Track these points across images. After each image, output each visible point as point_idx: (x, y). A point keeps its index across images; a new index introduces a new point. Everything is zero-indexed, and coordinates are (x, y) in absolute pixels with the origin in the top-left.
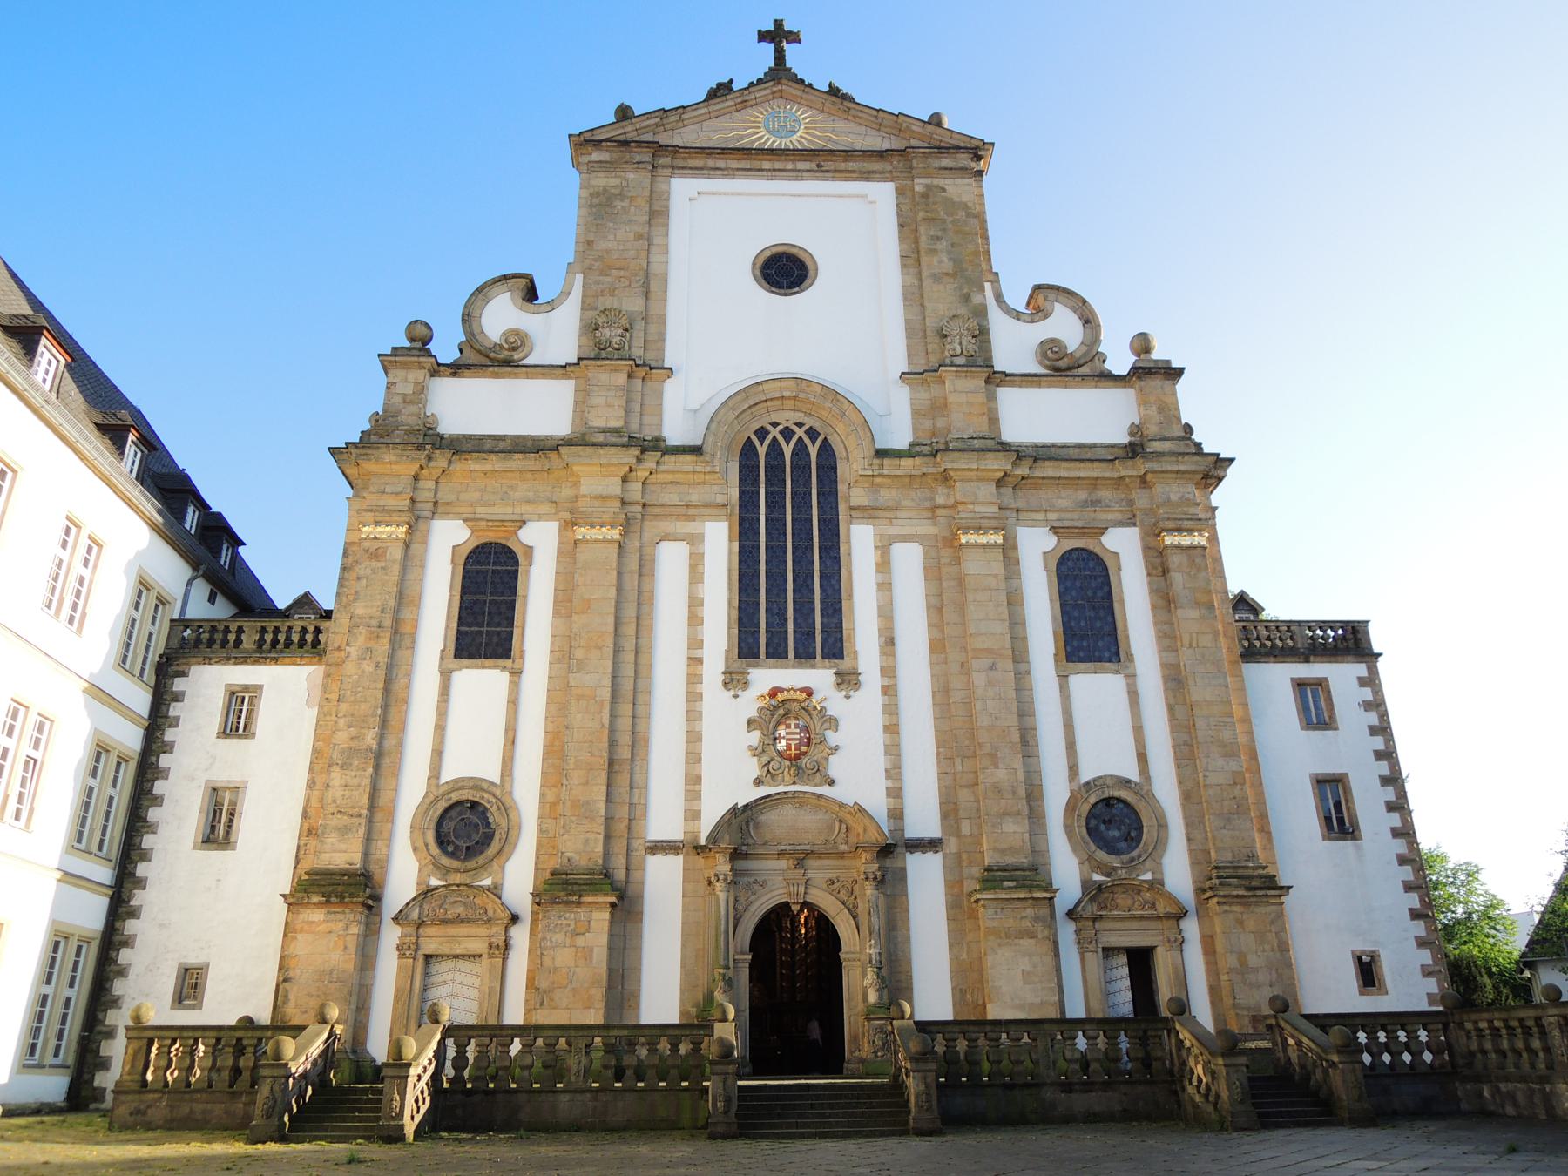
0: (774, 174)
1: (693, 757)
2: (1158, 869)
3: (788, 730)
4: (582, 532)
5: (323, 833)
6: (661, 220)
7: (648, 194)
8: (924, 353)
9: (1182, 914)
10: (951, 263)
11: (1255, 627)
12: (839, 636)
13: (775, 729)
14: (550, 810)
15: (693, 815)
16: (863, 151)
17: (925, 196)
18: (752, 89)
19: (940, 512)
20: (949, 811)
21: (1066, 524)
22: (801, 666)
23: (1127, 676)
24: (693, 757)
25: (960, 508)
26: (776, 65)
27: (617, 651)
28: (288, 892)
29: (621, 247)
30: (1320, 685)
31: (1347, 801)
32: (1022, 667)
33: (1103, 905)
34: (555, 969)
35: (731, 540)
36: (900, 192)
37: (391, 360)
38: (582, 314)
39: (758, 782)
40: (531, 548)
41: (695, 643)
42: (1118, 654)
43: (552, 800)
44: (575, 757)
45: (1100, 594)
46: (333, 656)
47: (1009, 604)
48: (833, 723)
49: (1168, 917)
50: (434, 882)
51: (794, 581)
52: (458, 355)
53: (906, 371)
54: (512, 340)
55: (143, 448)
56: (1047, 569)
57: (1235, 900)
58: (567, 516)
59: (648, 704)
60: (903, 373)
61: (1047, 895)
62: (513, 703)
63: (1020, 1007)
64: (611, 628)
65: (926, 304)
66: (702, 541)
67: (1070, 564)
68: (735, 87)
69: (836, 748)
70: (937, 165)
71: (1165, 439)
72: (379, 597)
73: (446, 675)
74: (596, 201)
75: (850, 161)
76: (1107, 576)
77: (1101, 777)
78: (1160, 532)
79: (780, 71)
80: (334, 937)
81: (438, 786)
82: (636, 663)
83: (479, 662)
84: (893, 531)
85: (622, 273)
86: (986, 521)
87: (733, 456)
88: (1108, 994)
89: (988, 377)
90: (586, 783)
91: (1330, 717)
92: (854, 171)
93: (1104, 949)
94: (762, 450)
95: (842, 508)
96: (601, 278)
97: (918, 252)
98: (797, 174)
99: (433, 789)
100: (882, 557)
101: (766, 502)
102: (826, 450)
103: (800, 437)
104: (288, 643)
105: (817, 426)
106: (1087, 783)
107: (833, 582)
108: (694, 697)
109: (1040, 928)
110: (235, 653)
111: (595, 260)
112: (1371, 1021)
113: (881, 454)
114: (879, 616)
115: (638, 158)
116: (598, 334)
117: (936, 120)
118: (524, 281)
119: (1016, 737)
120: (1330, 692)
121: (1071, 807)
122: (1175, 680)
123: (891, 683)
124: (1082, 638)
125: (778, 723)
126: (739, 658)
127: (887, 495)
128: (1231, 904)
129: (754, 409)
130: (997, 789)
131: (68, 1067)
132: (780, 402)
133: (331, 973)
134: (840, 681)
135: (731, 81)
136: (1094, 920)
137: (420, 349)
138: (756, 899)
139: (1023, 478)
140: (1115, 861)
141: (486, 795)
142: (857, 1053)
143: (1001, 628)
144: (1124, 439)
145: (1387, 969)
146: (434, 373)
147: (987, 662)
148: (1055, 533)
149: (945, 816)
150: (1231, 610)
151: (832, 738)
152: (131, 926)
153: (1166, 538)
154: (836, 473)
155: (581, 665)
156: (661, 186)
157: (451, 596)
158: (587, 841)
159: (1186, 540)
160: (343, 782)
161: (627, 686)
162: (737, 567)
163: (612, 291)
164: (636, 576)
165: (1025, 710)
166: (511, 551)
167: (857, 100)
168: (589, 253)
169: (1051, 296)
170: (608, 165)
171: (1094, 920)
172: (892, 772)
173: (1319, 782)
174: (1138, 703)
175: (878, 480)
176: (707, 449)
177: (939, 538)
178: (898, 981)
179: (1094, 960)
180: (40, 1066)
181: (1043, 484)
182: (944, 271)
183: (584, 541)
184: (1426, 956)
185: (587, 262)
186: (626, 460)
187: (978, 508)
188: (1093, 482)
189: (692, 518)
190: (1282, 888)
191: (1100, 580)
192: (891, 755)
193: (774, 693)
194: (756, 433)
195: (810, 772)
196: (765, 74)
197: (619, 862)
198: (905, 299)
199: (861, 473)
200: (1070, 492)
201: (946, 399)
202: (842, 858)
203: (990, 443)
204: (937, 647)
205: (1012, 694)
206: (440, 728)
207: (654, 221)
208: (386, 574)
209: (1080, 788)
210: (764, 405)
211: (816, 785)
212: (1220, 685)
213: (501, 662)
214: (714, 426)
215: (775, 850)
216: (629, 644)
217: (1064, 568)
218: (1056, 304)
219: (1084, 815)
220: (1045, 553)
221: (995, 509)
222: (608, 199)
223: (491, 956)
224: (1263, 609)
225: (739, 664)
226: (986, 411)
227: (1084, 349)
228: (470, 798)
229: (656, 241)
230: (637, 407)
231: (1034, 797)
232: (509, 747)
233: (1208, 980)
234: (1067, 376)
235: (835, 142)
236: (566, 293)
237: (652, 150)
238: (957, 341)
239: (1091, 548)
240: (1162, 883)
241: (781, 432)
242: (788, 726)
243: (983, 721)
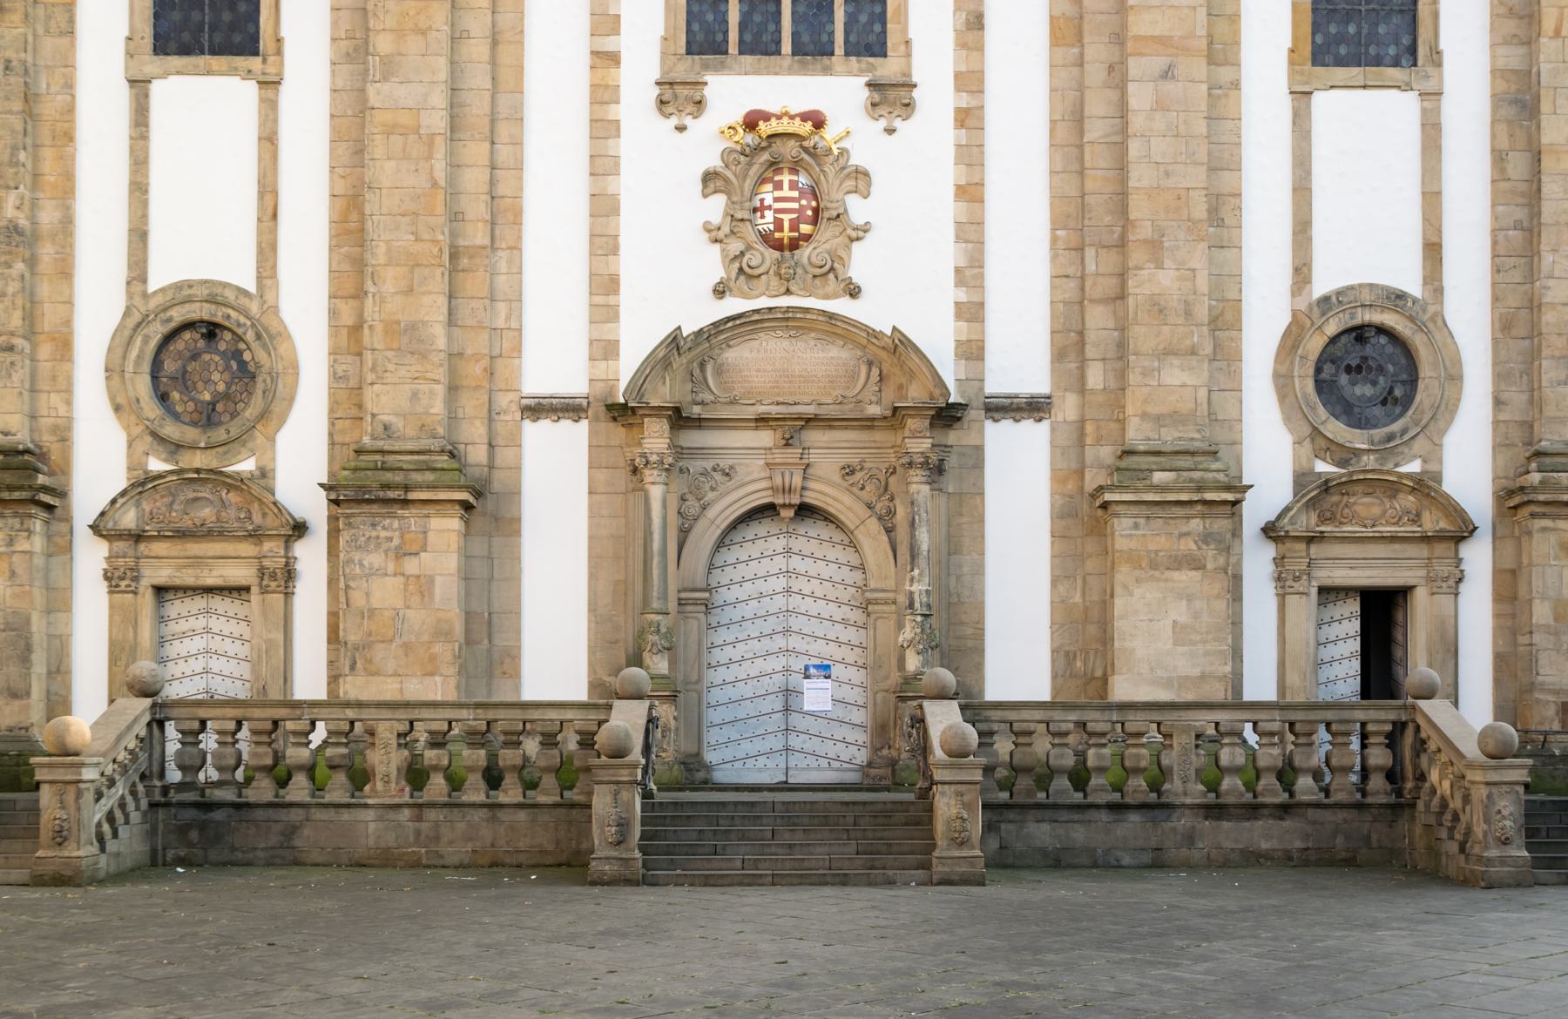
3: (778, 194)
13: (754, 193)
15: (605, 350)
22: (804, 70)
39: (720, 291)
43: (350, 323)
48: (861, 179)
69: (866, 228)
81: (145, 295)
90: (410, 291)
99: (138, 301)
121: (1291, 342)
140: (1357, 439)
141: (233, 314)
151: (858, 209)
158: (415, 395)
172: (968, 273)
197: (473, 434)
211: (827, 297)
225: (685, 68)
228: (206, 317)
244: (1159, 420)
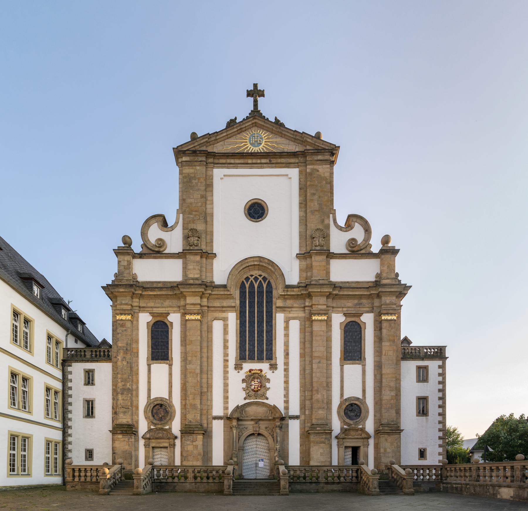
0: (252, 166)
1: (226, 391)
2: (364, 425)
4: (188, 317)
5: (119, 413)
6: (210, 189)
7: (204, 176)
8: (305, 246)
9: (369, 437)
10: (318, 206)
11: (408, 349)
12: (271, 352)
13: (251, 383)
14: (184, 407)
15: (226, 408)
16: (287, 153)
17: (311, 174)
18: (244, 122)
19: (306, 308)
20: (303, 407)
21: (349, 312)
22: (259, 362)
23: (362, 365)
24: (226, 391)
25: (313, 306)
26: (254, 109)
27: (201, 357)
28: (111, 429)
29: (196, 202)
30: (426, 368)
31: (426, 405)
32: (329, 362)
34: (188, 451)
35: (237, 319)
36: (300, 172)
37: (118, 252)
38: (183, 232)
39: (245, 399)
40: (172, 323)
41: (226, 355)
42: (361, 358)
43: (184, 404)
44: (190, 391)
45: (357, 337)
46: (114, 359)
47: (327, 341)
48: (268, 380)
49: (365, 438)
50: (152, 427)
51: (257, 334)
52: (141, 250)
53: (298, 253)
54: (159, 243)
55: (40, 288)
56: (341, 329)
57: (386, 434)
58: (182, 311)
59: (212, 375)
60: (297, 254)
61: (330, 432)
62: (170, 374)
63: (319, 462)
64: (199, 350)
65: (308, 224)
66: (227, 320)
67: (349, 327)
68: (237, 121)
69: (269, 388)
70: (316, 159)
71: (388, 279)
72: (125, 340)
73: (149, 366)
74: (185, 180)
75: (282, 158)
76: (361, 331)
77: (350, 397)
78: (381, 315)
79: (256, 113)
80: (125, 442)
81: (150, 400)
82: (207, 361)
83: (159, 361)
84: (291, 315)
85: (196, 213)
86: (322, 311)
87: (237, 288)
88: (345, 459)
89: (328, 255)
91: (426, 378)
92: (283, 163)
93: (345, 447)
94: (247, 286)
95: (274, 307)
96: (189, 215)
97: (306, 201)
98: (261, 166)
99: (149, 400)
100: (286, 325)
101: (249, 305)
102: (269, 284)
103: (260, 281)
104: (100, 356)
105: (266, 276)
106: (346, 399)
107: (270, 334)
108: (226, 372)
110: (84, 359)
111: (186, 208)
112: (423, 467)
113: (288, 287)
114: (284, 345)
115: (200, 159)
116: (189, 239)
117: (318, 136)
118: (162, 218)
119: (325, 385)
120: (428, 370)
121: (340, 406)
122: (378, 366)
123: (287, 367)
124: (350, 352)
125: (252, 381)
126: (240, 360)
127: (289, 303)
129: (244, 270)
130: (318, 401)
131: (60, 475)
132: (253, 267)
133: (126, 451)
134: (271, 367)
135: (236, 118)
136: (343, 439)
137: (128, 247)
138: (245, 432)
139: (336, 295)
140: (351, 422)
141: (165, 403)
142: (272, 473)
143: (323, 349)
144: (373, 279)
145: (428, 454)
146: (133, 258)
147: (318, 361)
148: (345, 316)
149: (301, 409)
150: (400, 343)
151: (268, 385)
152: (70, 439)
153: (382, 317)
154: (272, 294)
155: (190, 362)
156: (209, 173)
157: (148, 340)
158: (195, 416)
159: (390, 318)
160: (122, 398)
161: (205, 369)
162: (239, 329)
163: (193, 221)
164: (206, 332)
165: (329, 376)
166: (166, 324)
167: (286, 126)
168: (184, 204)
169: (355, 220)
170: (189, 163)
171: (343, 439)
172: (286, 395)
173: (419, 399)
174: (365, 374)
175: (286, 297)
176: (229, 286)
177: (306, 318)
179: (342, 450)
180: (51, 475)
181: (343, 297)
182: (315, 209)
183: (189, 320)
184: (441, 450)
185: (184, 208)
186: (201, 290)
187: (320, 307)
188: (360, 296)
189: (224, 311)
190: (401, 430)
191: (358, 332)
193: (250, 371)
194: (245, 279)
196: (250, 114)
197: (205, 422)
198: (300, 222)
199: (280, 294)
200: (352, 300)
201: (312, 264)
202: (270, 421)
203: (326, 282)
204: (303, 356)
205: (325, 371)
206: (149, 382)
207: (208, 189)
208: (127, 332)
209: (343, 401)
210: (248, 268)
211: (263, 400)
212: (392, 368)
213: (166, 361)
214: (230, 276)
215: (250, 418)
216: (205, 355)
217: (347, 328)
218: (356, 223)
219: (344, 408)
220: (341, 323)
221: (325, 307)
222: (190, 179)
223: (170, 447)
224: (412, 343)
225: (239, 362)
226: (325, 269)
227: (364, 242)
228: (160, 403)
229: (209, 198)
230: (204, 269)
231: (329, 403)
232: (170, 388)
233: (374, 455)
234: (356, 254)
235: (277, 148)
236: (177, 223)
237: (206, 155)
238: (318, 240)
239: (357, 321)
240: (365, 428)
241: (254, 279)
242: (255, 381)
243: (315, 379)
244: (318, 419)
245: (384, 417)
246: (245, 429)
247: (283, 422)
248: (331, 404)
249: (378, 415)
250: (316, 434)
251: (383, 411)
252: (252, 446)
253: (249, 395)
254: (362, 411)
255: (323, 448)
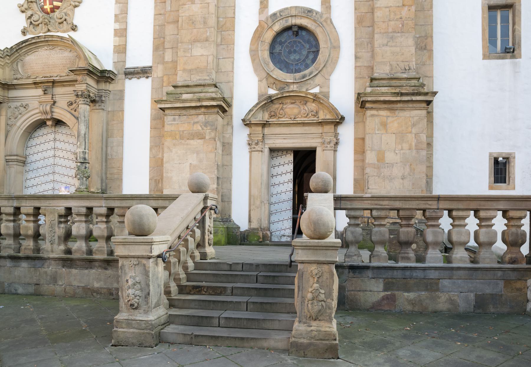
9: (339, 121)
33: (273, 114)
77: (287, 9)
106: (275, 14)
109: (208, 131)
121: (258, 35)
128: (378, 109)
130: (192, 21)
140: (288, 77)
149: (156, 48)
178: (111, 174)
192: (120, 3)
195: (60, 21)
209: (267, 19)
240: (327, 95)
244: (190, 71)
245: (379, 59)
246: (22, 109)
247: (111, 87)
248: (232, 29)
249: (366, 55)
250: (178, 112)
251: (379, 40)
252: (45, 154)
253: (31, 22)
254: (320, 47)
255: (198, 153)
